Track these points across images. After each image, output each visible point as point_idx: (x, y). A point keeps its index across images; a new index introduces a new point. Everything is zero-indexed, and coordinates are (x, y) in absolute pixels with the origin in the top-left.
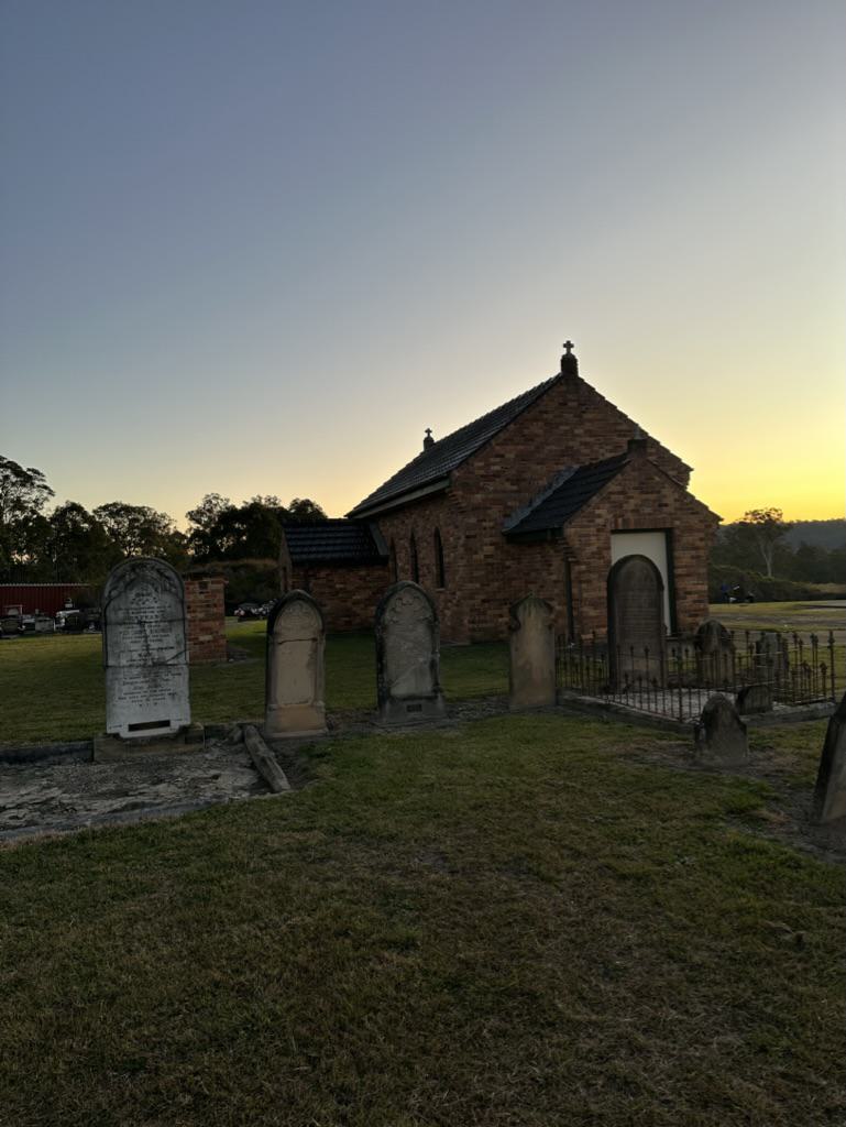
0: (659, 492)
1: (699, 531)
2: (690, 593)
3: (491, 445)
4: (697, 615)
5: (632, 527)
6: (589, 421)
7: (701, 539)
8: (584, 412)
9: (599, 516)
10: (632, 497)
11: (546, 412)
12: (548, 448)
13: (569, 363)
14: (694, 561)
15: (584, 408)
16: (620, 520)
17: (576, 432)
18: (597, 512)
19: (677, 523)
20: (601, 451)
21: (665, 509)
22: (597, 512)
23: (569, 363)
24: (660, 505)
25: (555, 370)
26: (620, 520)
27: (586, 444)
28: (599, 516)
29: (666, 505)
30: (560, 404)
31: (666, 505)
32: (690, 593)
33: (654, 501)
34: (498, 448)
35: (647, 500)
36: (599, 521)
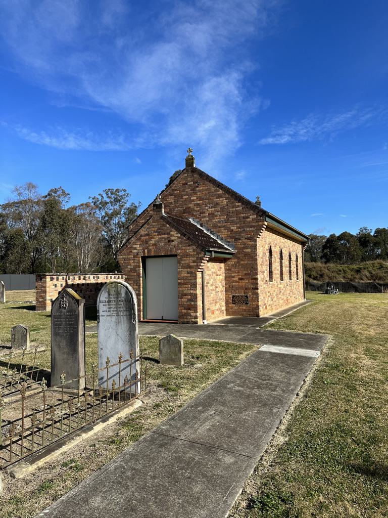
0: (168, 233)
1: (192, 256)
2: (186, 295)
3: (147, 211)
4: (189, 309)
5: (153, 254)
6: (200, 191)
7: (194, 262)
8: (197, 187)
9: (135, 249)
10: (153, 238)
11: (176, 190)
12: (177, 209)
13: (190, 162)
14: (189, 275)
15: (197, 184)
16: (146, 251)
17: (192, 199)
18: (135, 246)
19: (180, 251)
20: (207, 208)
21: (172, 243)
22: (135, 246)
23: (190, 162)
24: (169, 241)
25: (183, 166)
26: (146, 251)
27: (198, 205)
28: (135, 249)
29: (173, 241)
30: (183, 184)
31: (173, 241)
32: (186, 295)
33: (165, 239)
34: (151, 212)
35: (161, 238)
36: (135, 251)
